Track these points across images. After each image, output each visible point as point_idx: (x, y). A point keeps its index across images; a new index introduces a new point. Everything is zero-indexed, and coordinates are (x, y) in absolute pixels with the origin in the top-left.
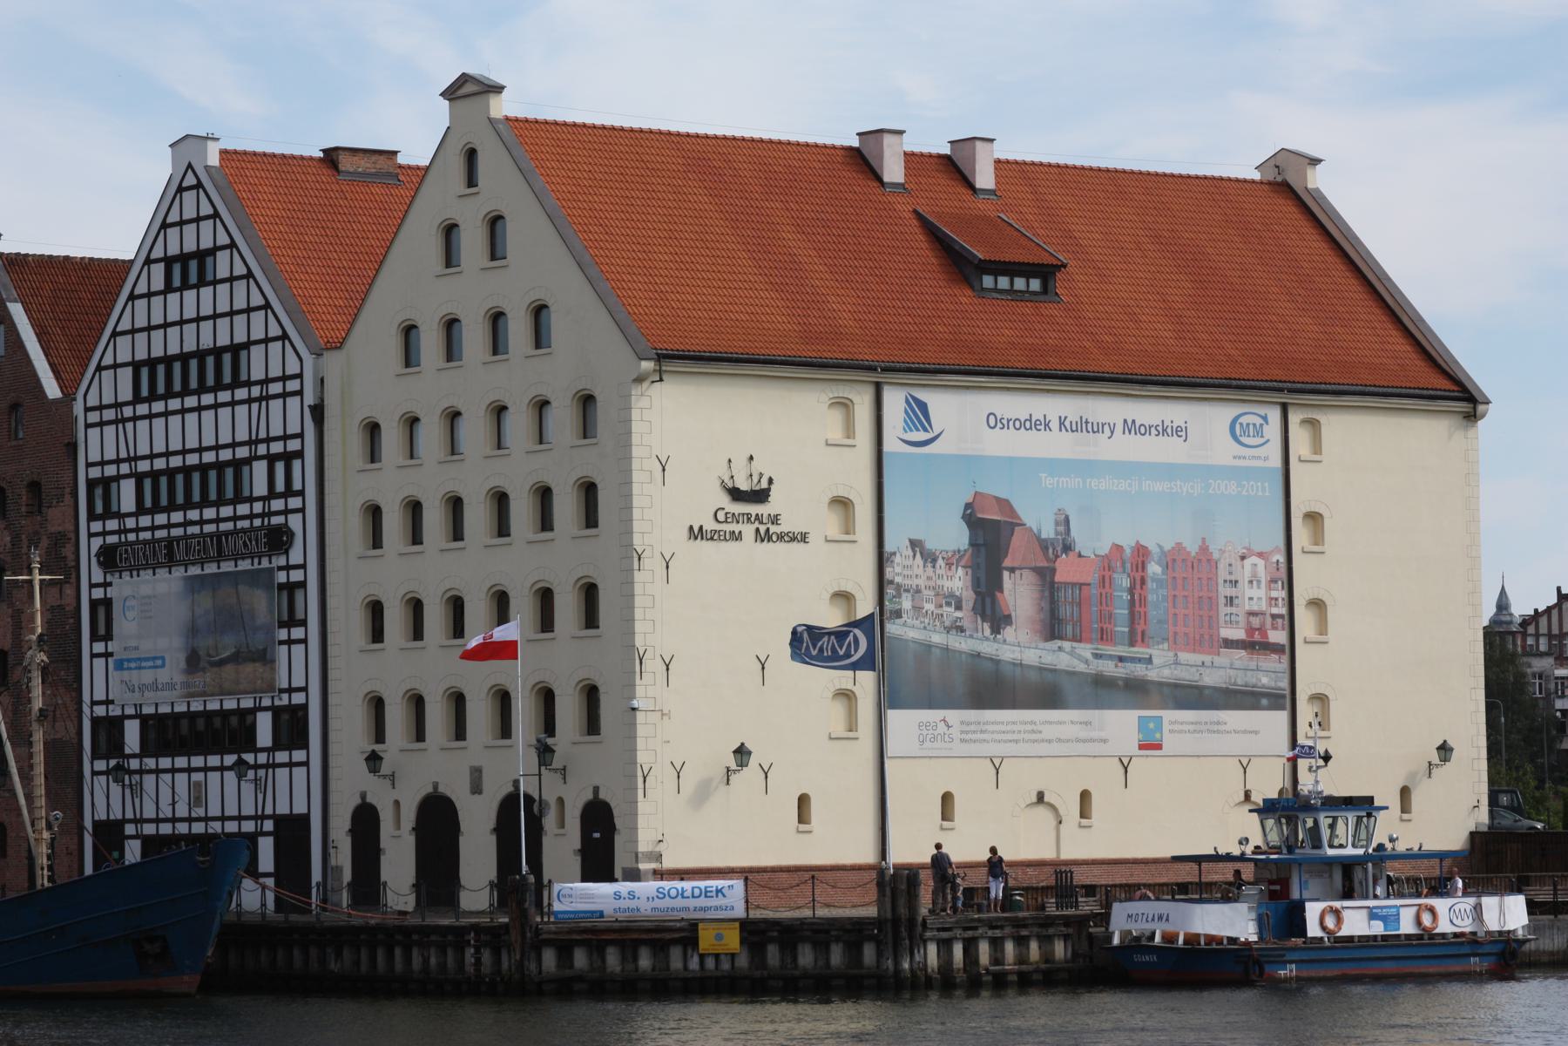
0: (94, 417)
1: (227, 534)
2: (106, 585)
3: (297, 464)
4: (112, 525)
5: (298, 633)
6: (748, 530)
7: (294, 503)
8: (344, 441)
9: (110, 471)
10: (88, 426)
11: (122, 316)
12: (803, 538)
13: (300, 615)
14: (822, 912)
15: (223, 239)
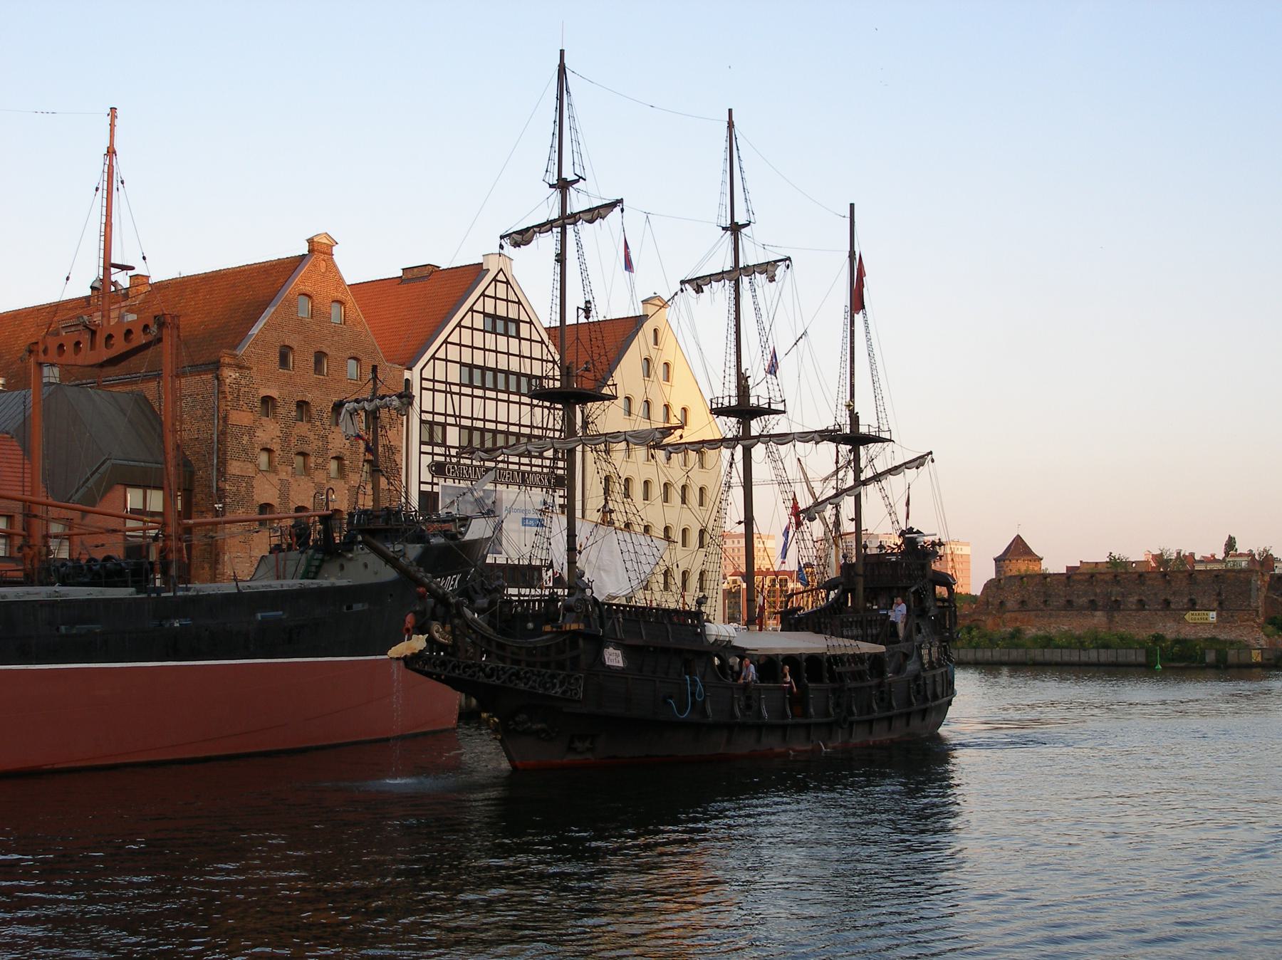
0: (426, 384)
2: (432, 484)
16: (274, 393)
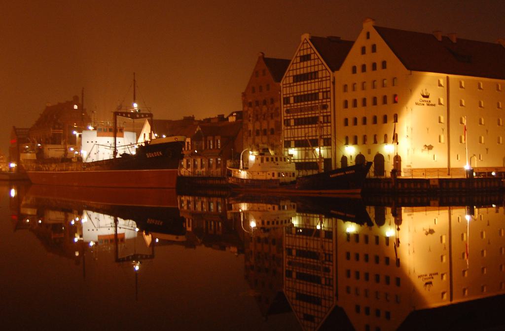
0: (284, 86)
1: (313, 106)
2: (287, 116)
3: (329, 93)
4: (288, 105)
5: (329, 124)
6: (425, 103)
7: (328, 100)
8: (339, 88)
9: (288, 96)
10: (283, 88)
11: (290, 67)
12: (434, 105)
13: (329, 121)
14: (414, 178)
15: (312, 52)
16: (250, 100)
